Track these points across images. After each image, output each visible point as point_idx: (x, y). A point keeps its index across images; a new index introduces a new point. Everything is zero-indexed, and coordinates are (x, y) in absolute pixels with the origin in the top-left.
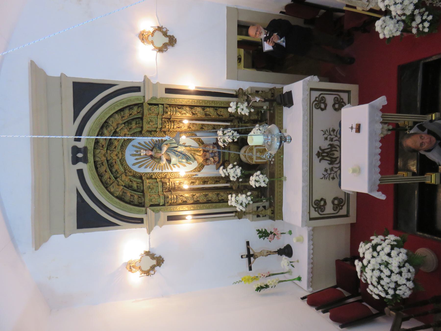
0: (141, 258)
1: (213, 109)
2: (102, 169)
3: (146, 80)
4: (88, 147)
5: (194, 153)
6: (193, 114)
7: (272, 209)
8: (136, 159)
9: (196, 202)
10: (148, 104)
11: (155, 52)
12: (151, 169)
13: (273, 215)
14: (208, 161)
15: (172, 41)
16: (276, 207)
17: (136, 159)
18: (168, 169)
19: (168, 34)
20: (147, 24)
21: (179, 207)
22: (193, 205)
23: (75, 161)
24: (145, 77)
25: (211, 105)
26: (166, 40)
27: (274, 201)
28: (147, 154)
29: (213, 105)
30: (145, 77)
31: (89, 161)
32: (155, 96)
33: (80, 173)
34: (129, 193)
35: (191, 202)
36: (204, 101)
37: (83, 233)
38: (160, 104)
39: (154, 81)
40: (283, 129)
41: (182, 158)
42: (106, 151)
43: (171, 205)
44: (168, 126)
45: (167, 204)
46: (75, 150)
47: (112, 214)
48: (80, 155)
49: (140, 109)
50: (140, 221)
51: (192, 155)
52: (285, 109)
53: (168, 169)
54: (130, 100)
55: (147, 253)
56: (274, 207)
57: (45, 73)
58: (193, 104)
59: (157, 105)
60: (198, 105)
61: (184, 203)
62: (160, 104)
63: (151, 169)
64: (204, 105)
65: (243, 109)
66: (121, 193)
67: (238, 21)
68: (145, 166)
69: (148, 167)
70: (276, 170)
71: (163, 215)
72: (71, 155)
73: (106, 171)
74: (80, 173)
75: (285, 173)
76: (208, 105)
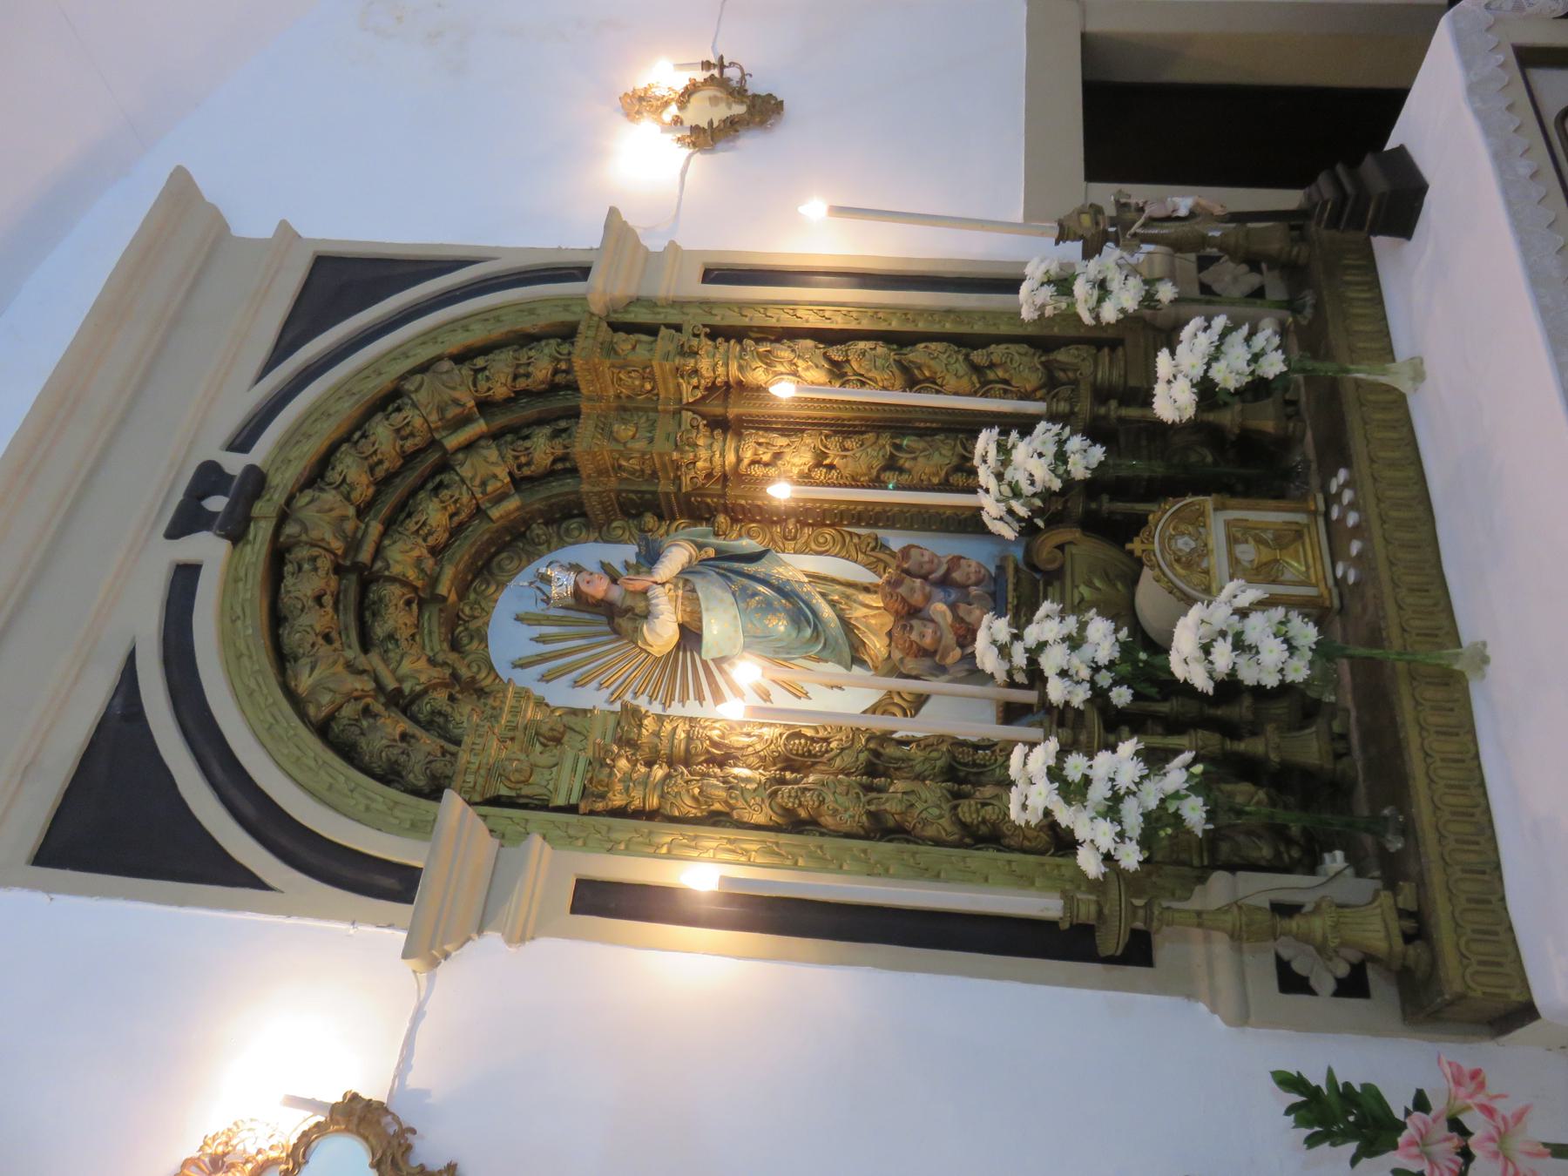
0: (306, 1142)
1: (940, 346)
2: (302, 586)
3: (616, 227)
4: (271, 472)
5: (848, 597)
6: (837, 371)
7: (1407, 898)
8: (542, 639)
9: (795, 824)
10: (610, 325)
11: (687, 151)
12: (605, 693)
13: (1415, 951)
14: (915, 623)
15: (761, 111)
16: (1436, 878)
17: (542, 639)
18: (700, 698)
19: (750, 93)
20: (667, 74)
21: (667, 836)
22: (770, 837)
23: (188, 520)
24: (613, 212)
25: (936, 328)
26: (739, 109)
27: (1408, 830)
28: (584, 587)
29: (949, 327)
30: (613, 212)
31: (251, 537)
32: (644, 293)
33: (185, 577)
34: (392, 725)
35: (759, 818)
36: (894, 309)
37: (49, 889)
38: (668, 326)
39: (655, 244)
40: (1394, 360)
41: (767, 607)
42: (386, 559)
43: (620, 813)
44: (712, 454)
45: (597, 809)
46: (209, 478)
47: (249, 810)
48: (217, 504)
49: (565, 348)
50: (389, 882)
51: (833, 604)
52: (1381, 244)
53: (700, 698)
54: (532, 312)
55: (356, 1115)
56: (1421, 884)
57: (226, 227)
58: (839, 323)
59: (652, 330)
60: (866, 325)
61: (716, 819)
62: (668, 326)
63: (605, 693)
64: (895, 325)
65: (1102, 286)
66: (348, 711)
67: (1084, 36)
68: (574, 675)
69: (594, 684)
70: (1391, 610)
71: (550, 864)
72: (178, 496)
73: (318, 599)
74: (185, 577)
75: (1471, 624)
76: (922, 326)
